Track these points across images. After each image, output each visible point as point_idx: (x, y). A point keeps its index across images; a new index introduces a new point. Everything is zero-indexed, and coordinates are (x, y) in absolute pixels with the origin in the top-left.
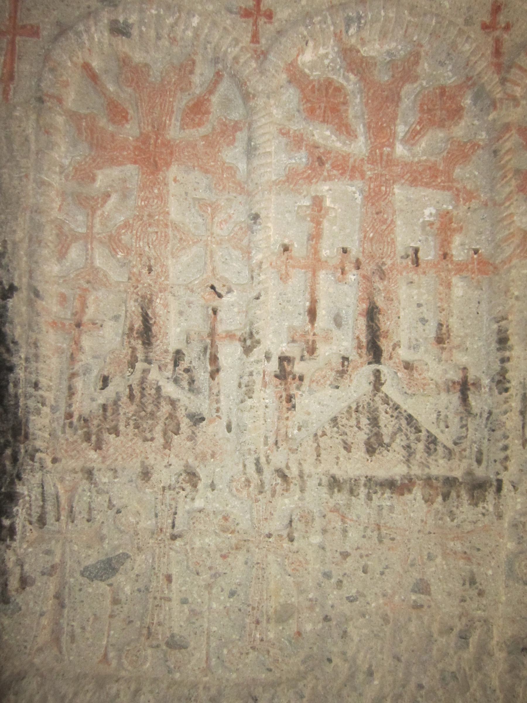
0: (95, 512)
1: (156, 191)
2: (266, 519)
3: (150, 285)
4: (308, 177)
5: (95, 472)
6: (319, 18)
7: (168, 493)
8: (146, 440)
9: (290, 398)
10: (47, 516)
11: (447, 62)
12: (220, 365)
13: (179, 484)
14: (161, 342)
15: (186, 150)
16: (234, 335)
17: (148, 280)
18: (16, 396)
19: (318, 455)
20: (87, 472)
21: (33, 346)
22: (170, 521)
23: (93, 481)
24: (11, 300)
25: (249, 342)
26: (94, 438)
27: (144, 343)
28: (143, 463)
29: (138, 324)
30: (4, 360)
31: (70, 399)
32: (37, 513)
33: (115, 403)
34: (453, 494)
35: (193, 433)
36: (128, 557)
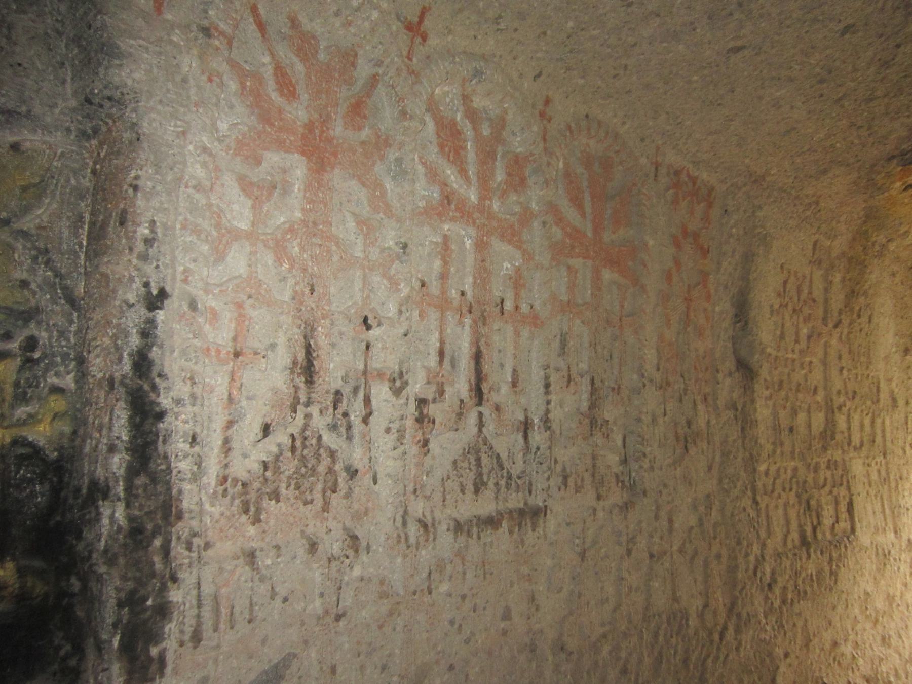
0: (257, 608)
2: (412, 575)
3: (312, 309)
5: (258, 553)
7: (334, 564)
8: (306, 503)
9: (426, 443)
10: (204, 627)
12: (374, 408)
13: (344, 552)
16: (384, 374)
17: (310, 302)
18: (166, 457)
19: (444, 501)
20: (249, 556)
21: (189, 382)
22: (335, 599)
23: (255, 566)
24: (161, 312)
25: (398, 384)
26: (252, 509)
27: (306, 382)
28: (302, 532)
29: (301, 356)
30: (153, 403)
31: (226, 457)
32: (191, 626)
33: (277, 458)
34: (524, 523)
35: (350, 489)
36: (295, 655)
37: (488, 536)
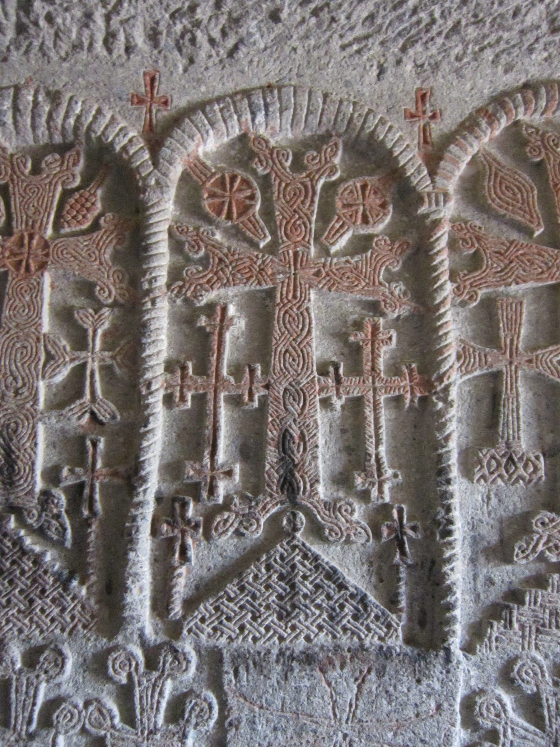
1: (28, 298)
4: (208, 282)
6: (222, 105)
11: (369, 153)
14: (25, 481)
15: (65, 252)
37: (301, 678)
